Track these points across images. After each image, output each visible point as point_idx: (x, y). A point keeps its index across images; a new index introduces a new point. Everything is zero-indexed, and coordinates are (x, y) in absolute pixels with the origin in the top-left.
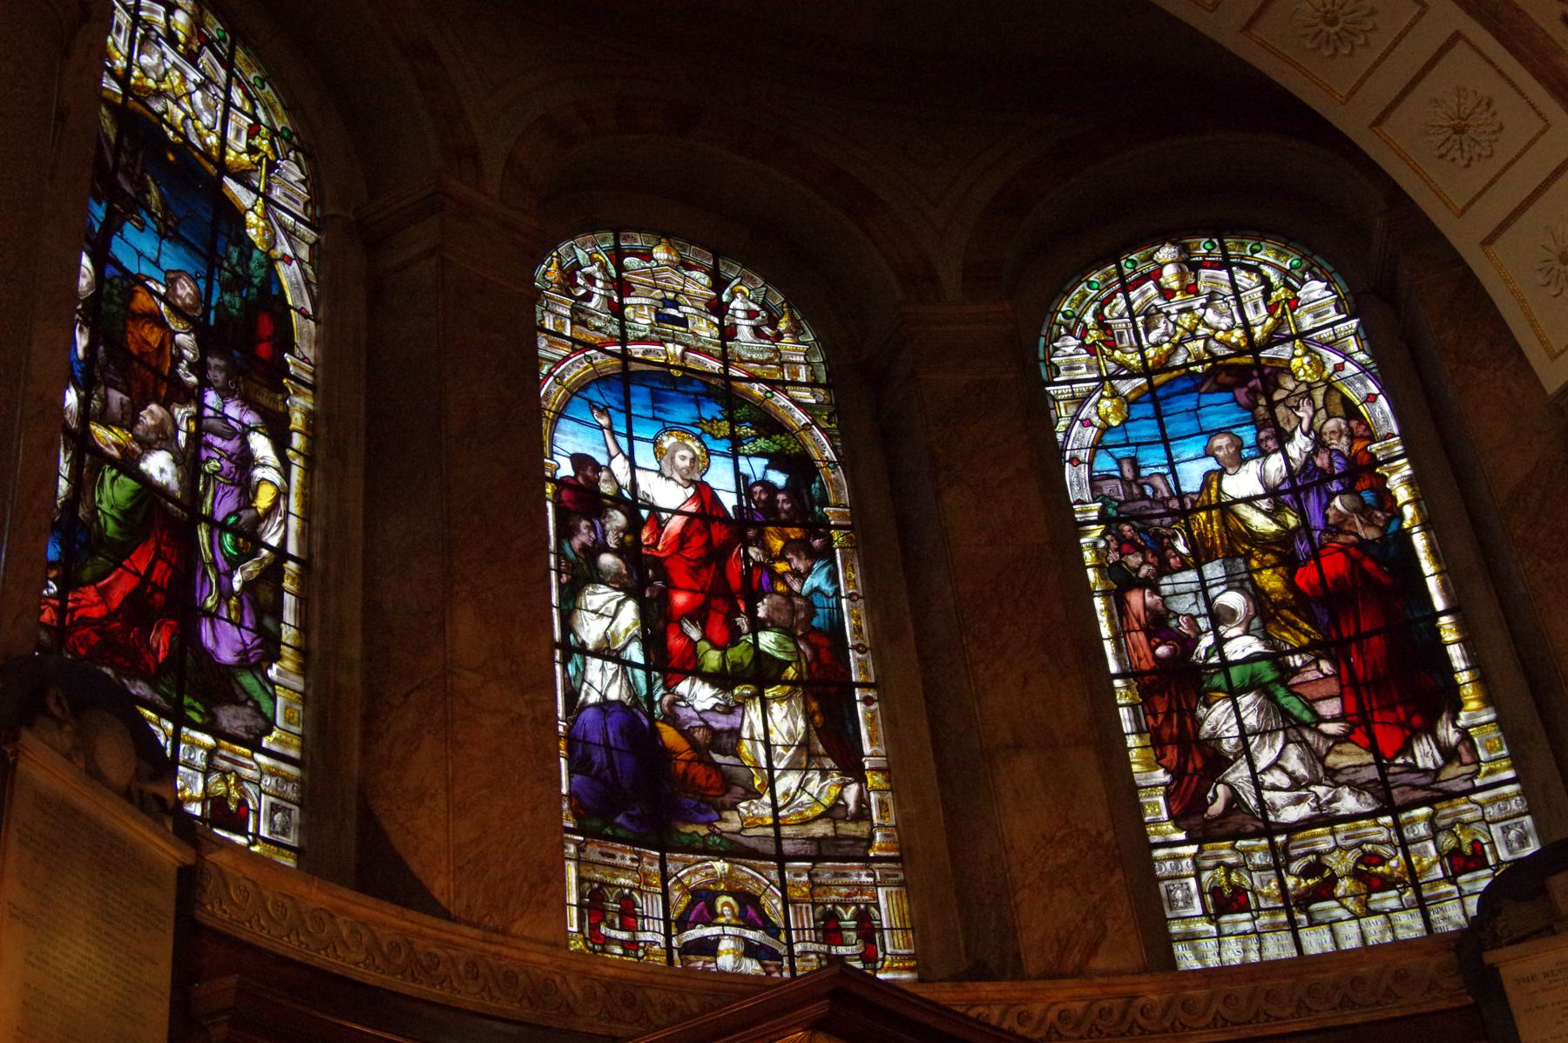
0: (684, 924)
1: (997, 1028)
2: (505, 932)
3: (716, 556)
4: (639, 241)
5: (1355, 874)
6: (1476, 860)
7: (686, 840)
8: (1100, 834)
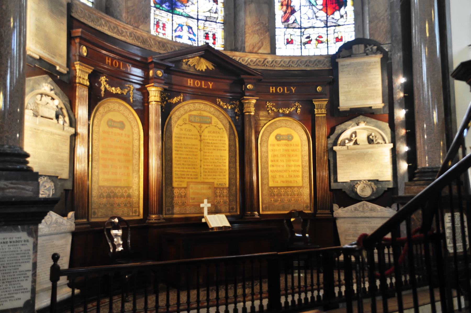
0: (176, 31)
1: (238, 62)
2: (138, 27)
5: (317, 40)
6: (341, 40)
7: (178, 13)
8: (266, 24)
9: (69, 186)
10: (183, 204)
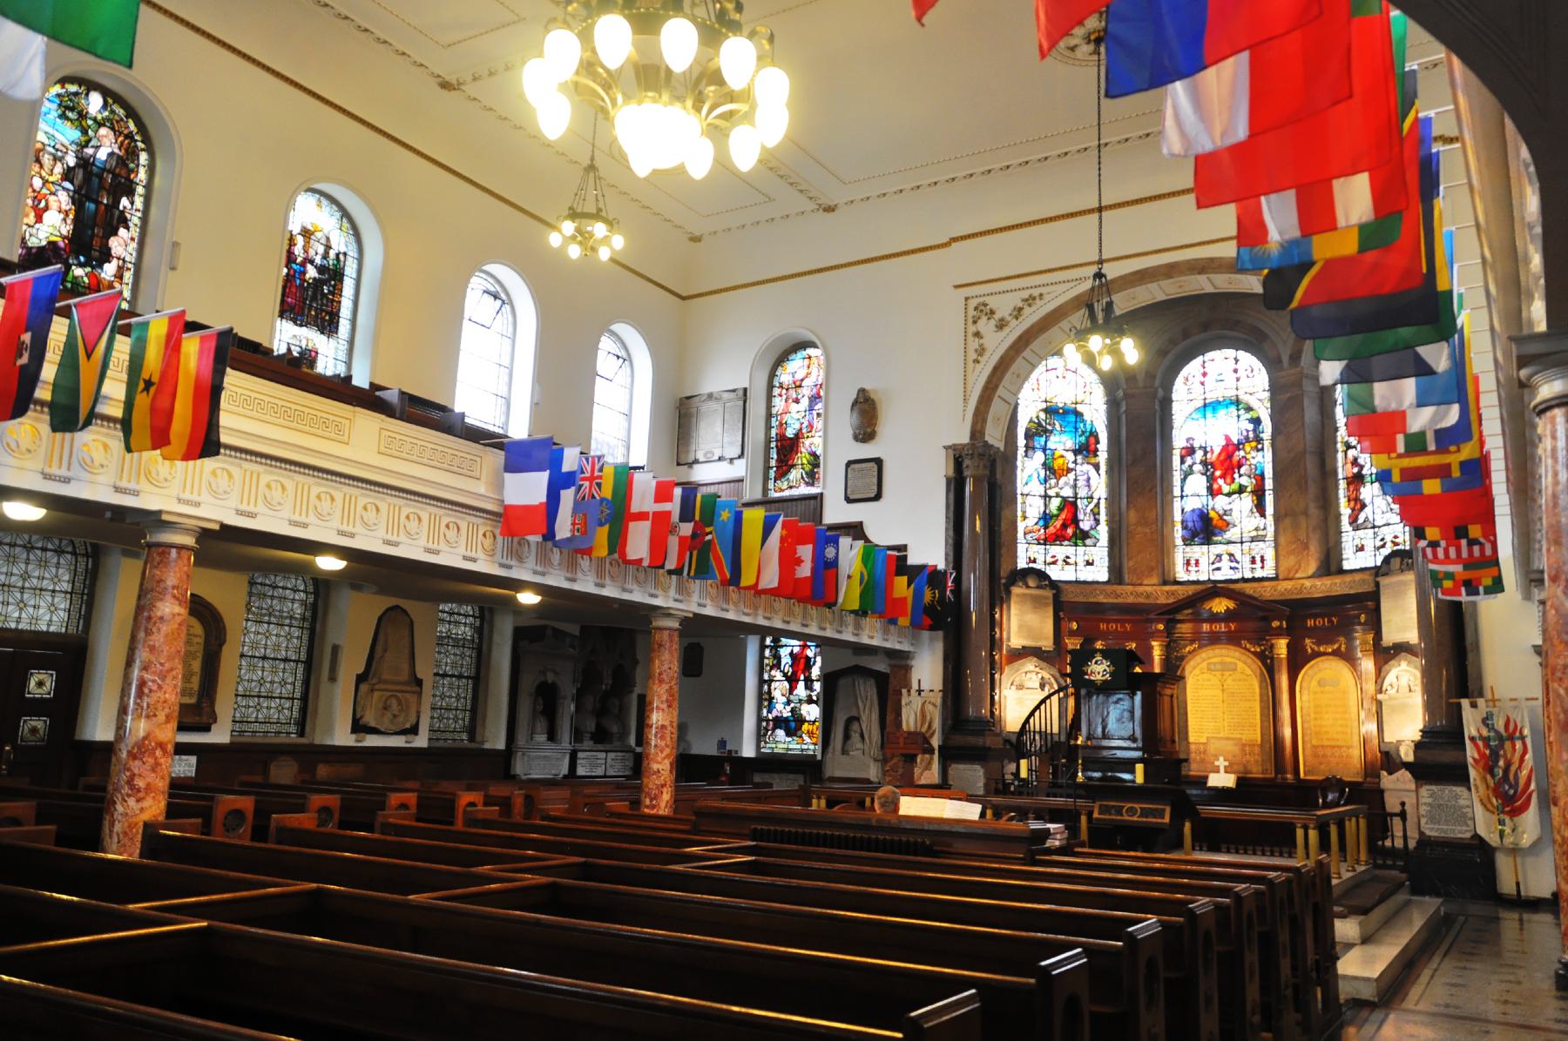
3: (1230, 456)
4: (1209, 355)
10: (1202, 761)
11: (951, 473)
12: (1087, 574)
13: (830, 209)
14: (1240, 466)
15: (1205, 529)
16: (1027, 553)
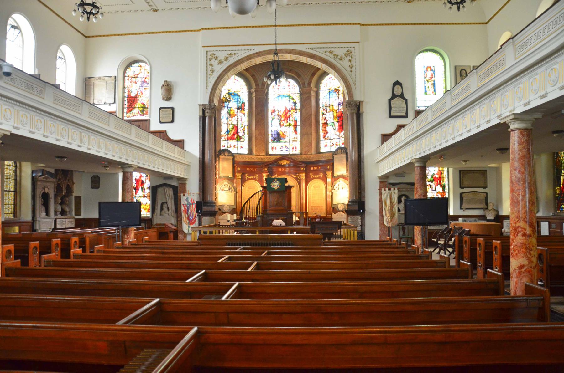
3: (286, 114)
9: (235, 207)
11: (201, 114)
12: (241, 151)
13: (156, 11)
14: (289, 117)
15: (278, 137)
16: (225, 144)
